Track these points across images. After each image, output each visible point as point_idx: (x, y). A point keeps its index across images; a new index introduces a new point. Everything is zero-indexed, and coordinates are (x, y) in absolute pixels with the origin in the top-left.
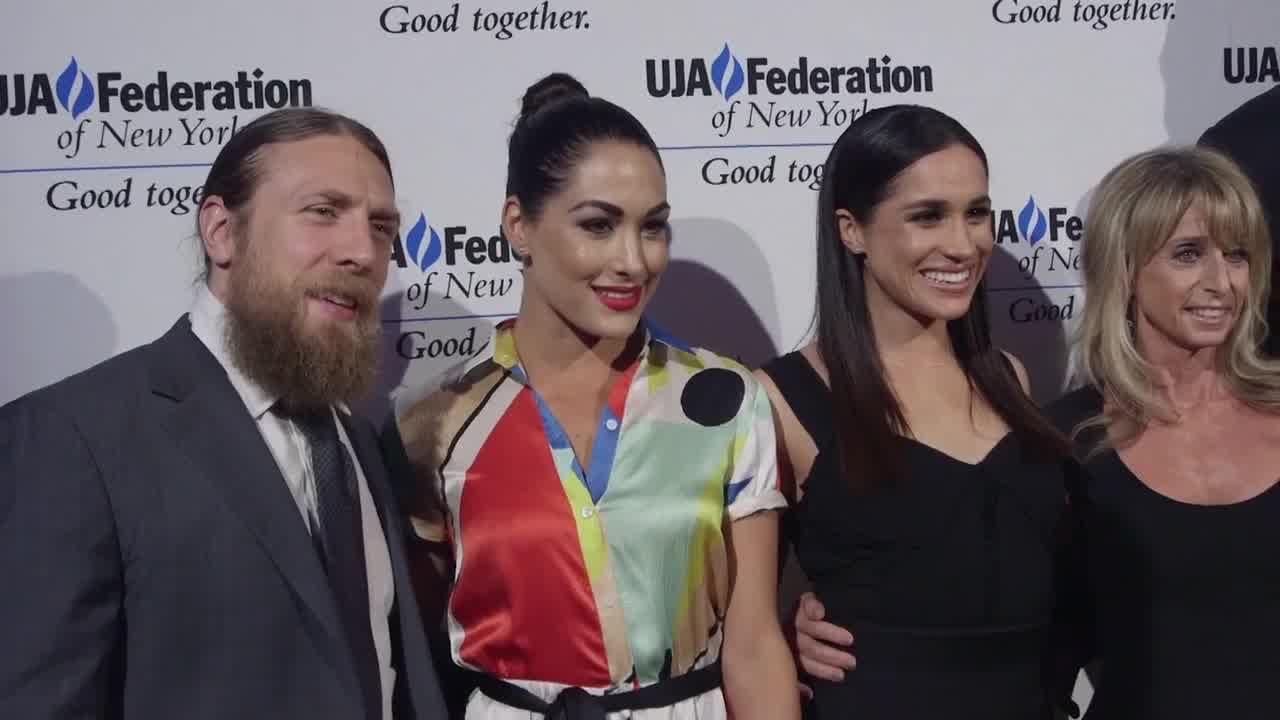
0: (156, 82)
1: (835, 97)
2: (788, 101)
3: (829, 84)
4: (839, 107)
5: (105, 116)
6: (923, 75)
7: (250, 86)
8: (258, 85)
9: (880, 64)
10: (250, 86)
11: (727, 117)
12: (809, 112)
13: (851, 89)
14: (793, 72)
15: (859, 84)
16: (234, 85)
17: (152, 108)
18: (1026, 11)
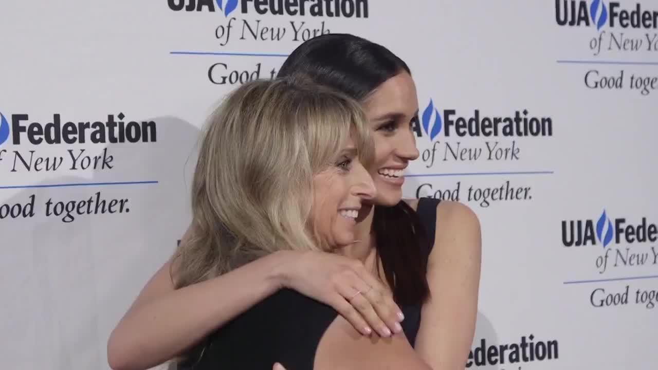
0: (53, 122)
1: (82, 146)
2: (45, 150)
3: (77, 136)
4: (498, 146)
5: (17, 147)
6: (149, 128)
7: (116, 126)
8: (122, 124)
9: (117, 120)
10: (116, 126)
11: (431, 152)
12: (61, 159)
13: (94, 140)
14: (49, 126)
15: (101, 136)
16: (105, 125)
17: (49, 141)
18: (234, 76)
